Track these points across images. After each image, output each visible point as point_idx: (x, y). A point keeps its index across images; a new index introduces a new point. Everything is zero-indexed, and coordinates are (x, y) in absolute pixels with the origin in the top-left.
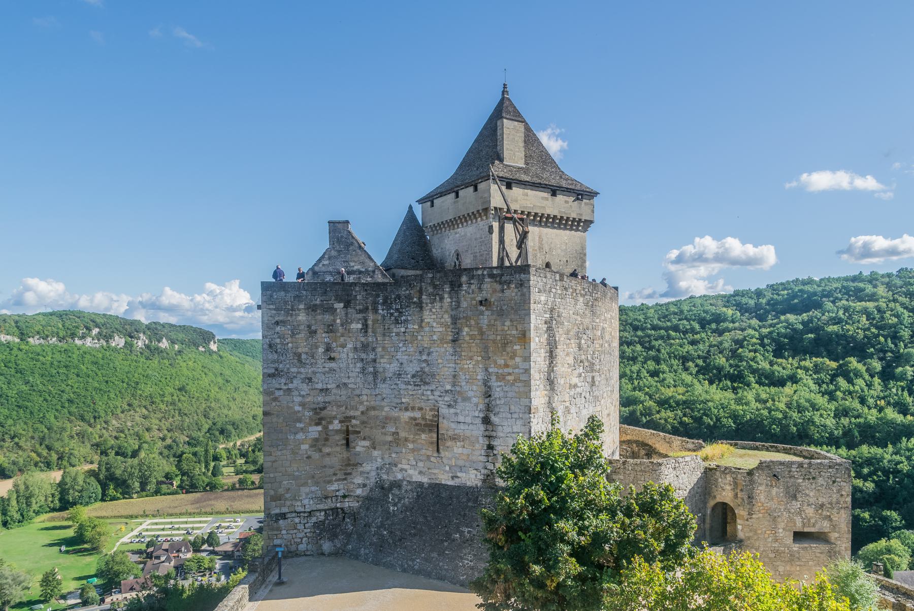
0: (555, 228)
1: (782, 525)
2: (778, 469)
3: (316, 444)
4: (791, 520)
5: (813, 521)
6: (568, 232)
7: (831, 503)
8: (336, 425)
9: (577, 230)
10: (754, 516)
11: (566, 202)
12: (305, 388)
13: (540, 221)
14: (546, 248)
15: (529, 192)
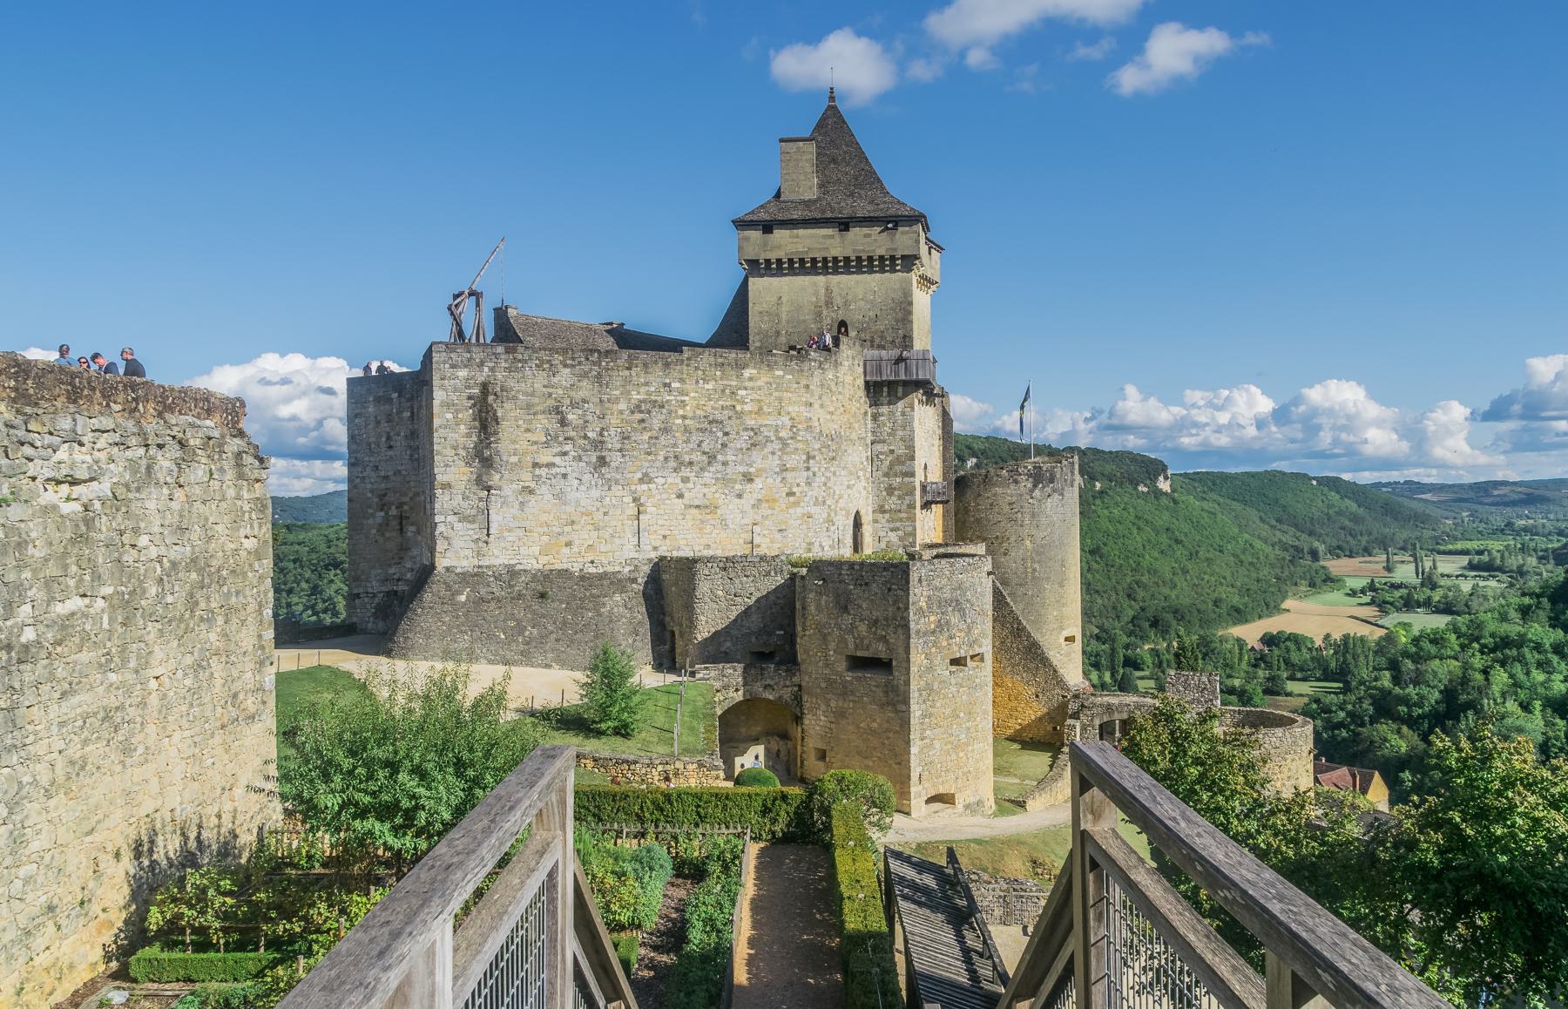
1: (832, 645)
2: (827, 571)
3: (383, 527)
4: (843, 640)
7: (886, 619)
8: (394, 512)
9: (893, 271)
11: (867, 236)
12: (373, 474)
14: (838, 300)
15: (801, 232)
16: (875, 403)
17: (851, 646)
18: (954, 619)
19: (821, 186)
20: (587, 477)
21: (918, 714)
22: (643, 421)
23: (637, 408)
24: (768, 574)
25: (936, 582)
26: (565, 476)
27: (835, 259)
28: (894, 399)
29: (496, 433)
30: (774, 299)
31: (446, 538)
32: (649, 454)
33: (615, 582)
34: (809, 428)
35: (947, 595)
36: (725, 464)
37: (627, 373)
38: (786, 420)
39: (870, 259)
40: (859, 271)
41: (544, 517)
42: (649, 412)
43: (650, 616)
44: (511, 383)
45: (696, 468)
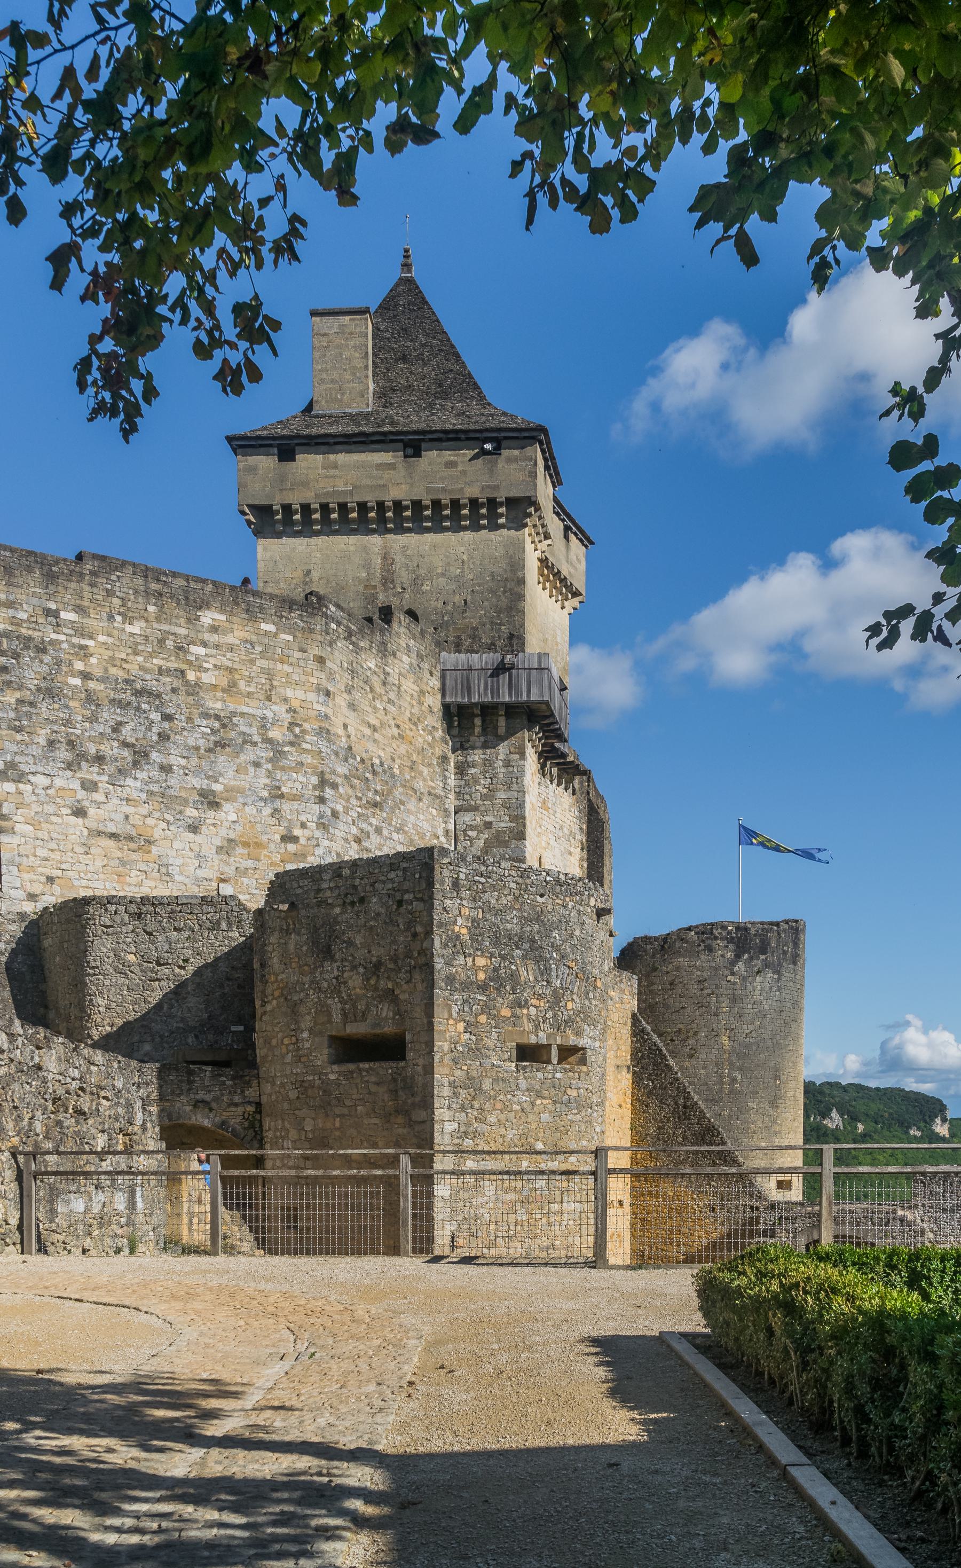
0: (428, 530)
4: (324, 1010)
5: (361, 1006)
6: (467, 536)
9: (494, 526)
10: (269, 1008)
13: (382, 519)
16: (461, 746)
17: (337, 1017)
18: (527, 974)
19: (379, 396)
21: (450, 1127)
24: (215, 926)
25: (490, 897)
27: (398, 505)
28: (492, 738)
30: (299, 573)
32: (19, 730)
34: (325, 733)
35: (513, 925)
36: (166, 769)
38: (280, 710)
39: (456, 504)
40: (438, 528)
45: (110, 768)
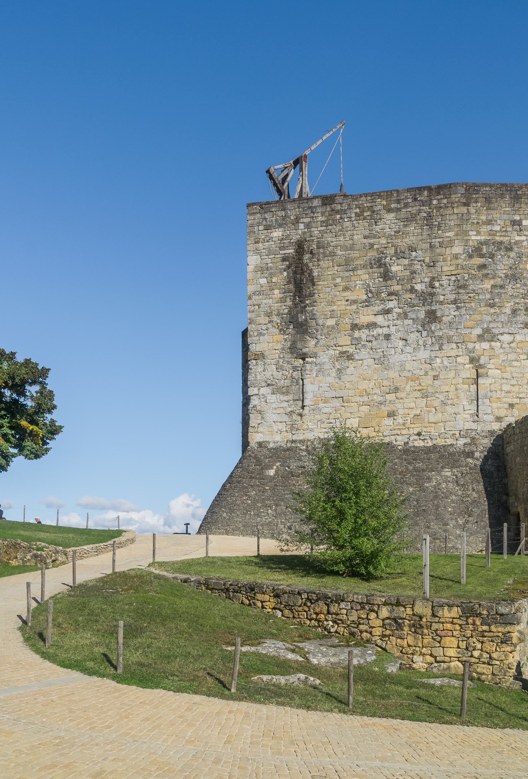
20: (413, 337)
22: (483, 266)
23: (477, 251)
26: (387, 337)
29: (311, 295)
31: (260, 412)
32: (492, 306)
33: (444, 456)
37: (464, 209)
41: (363, 385)
42: (492, 256)
43: (489, 495)
44: (329, 238)
